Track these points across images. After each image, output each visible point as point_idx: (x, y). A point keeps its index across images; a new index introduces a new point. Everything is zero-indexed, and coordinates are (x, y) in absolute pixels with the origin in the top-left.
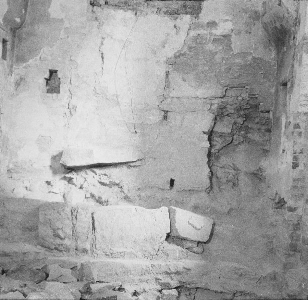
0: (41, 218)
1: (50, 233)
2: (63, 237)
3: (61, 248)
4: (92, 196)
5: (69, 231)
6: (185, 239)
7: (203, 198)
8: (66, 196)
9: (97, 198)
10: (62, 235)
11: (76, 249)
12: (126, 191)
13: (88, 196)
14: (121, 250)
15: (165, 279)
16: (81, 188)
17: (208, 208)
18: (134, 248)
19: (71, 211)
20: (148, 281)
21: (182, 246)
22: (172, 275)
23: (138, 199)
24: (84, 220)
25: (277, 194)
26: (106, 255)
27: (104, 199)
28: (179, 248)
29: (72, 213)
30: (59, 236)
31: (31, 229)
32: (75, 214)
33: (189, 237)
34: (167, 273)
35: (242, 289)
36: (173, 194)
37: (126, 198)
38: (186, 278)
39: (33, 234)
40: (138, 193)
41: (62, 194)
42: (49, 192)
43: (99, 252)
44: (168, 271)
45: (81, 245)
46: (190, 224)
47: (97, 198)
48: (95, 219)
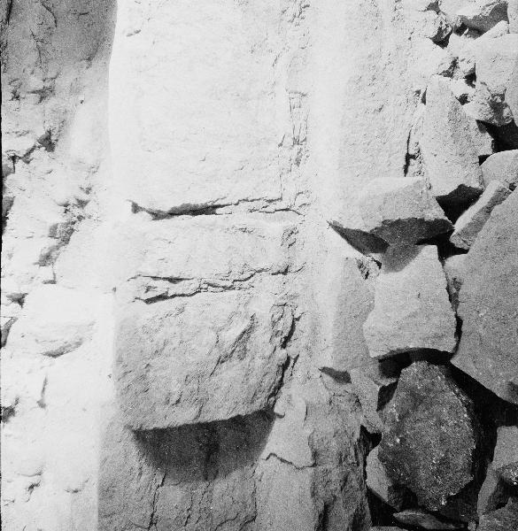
0: (184, 416)
1: (231, 373)
2: (247, 323)
3: (284, 326)
4: (46, 259)
5: (225, 303)
8: (54, 348)
9: (54, 242)
10: (235, 331)
11: (285, 272)
12: (28, 143)
13: (46, 272)
14: (282, 100)
16: (20, 300)
18: (272, 57)
19: (149, 301)
23: (51, 103)
24: (191, 249)
26: (298, 163)
27: (59, 219)
29: (162, 297)
30: (247, 333)
31: (199, 448)
32: (162, 287)
37: (48, 143)
39: (227, 439)
41: (49, 360)
42: (42, 405)
43: (291, 190)
45: (274, 256)
47: (54, 242)
48: (178, 204)
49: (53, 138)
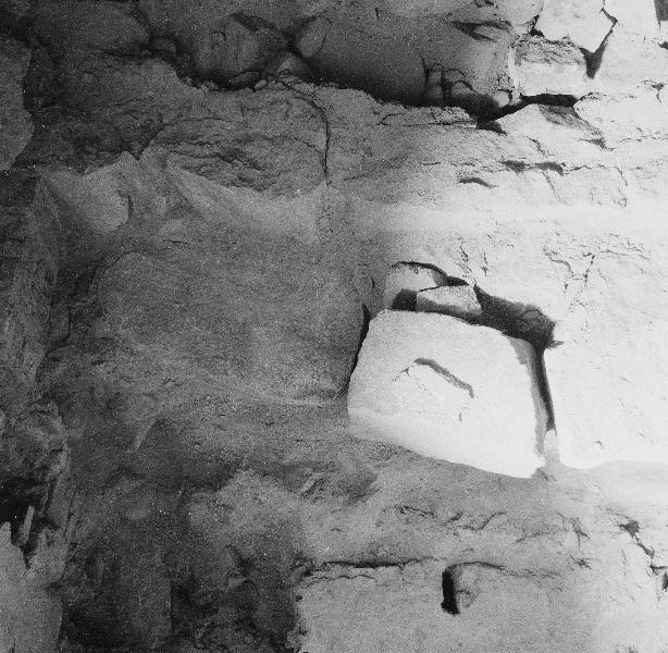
6: (471, 319)
7: (325, 529)
15: (559, 139)
17: (310, 491)
20: (638, 135)
21: (481, 296)
22: (535, 158)
23: (587, 524)
25: (28, 550)
28: (491, 290)
33: (463, 327)
34: (557, 168)
35: (230, 100)
36: (446, 548)
38: (478, 144)
40: (587, 549)
44: (553, 174)
46: (463, 385)
49: (625, 522)
